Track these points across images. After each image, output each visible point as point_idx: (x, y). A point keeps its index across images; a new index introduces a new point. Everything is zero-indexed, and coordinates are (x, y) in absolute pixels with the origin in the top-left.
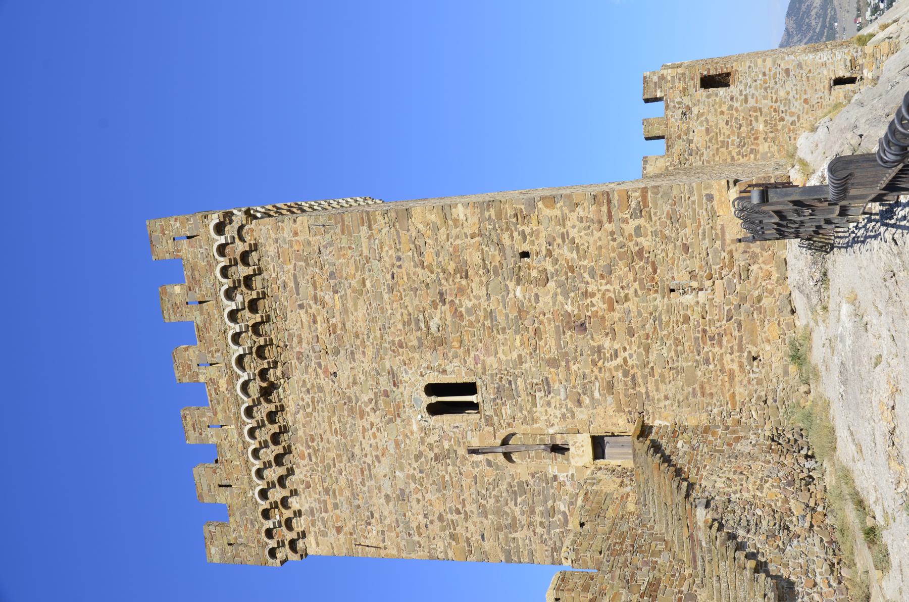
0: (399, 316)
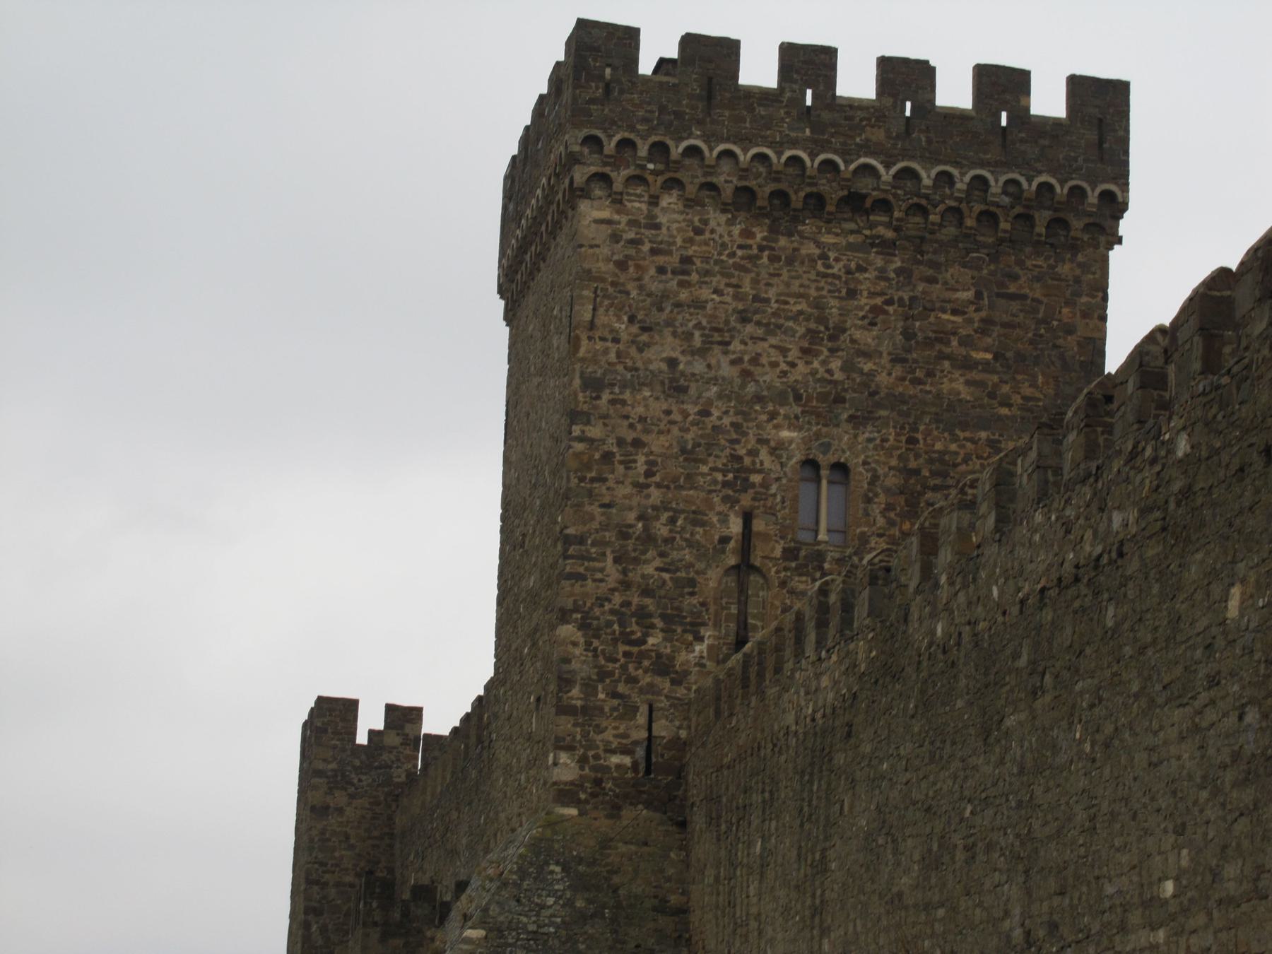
0: (953, 447)
